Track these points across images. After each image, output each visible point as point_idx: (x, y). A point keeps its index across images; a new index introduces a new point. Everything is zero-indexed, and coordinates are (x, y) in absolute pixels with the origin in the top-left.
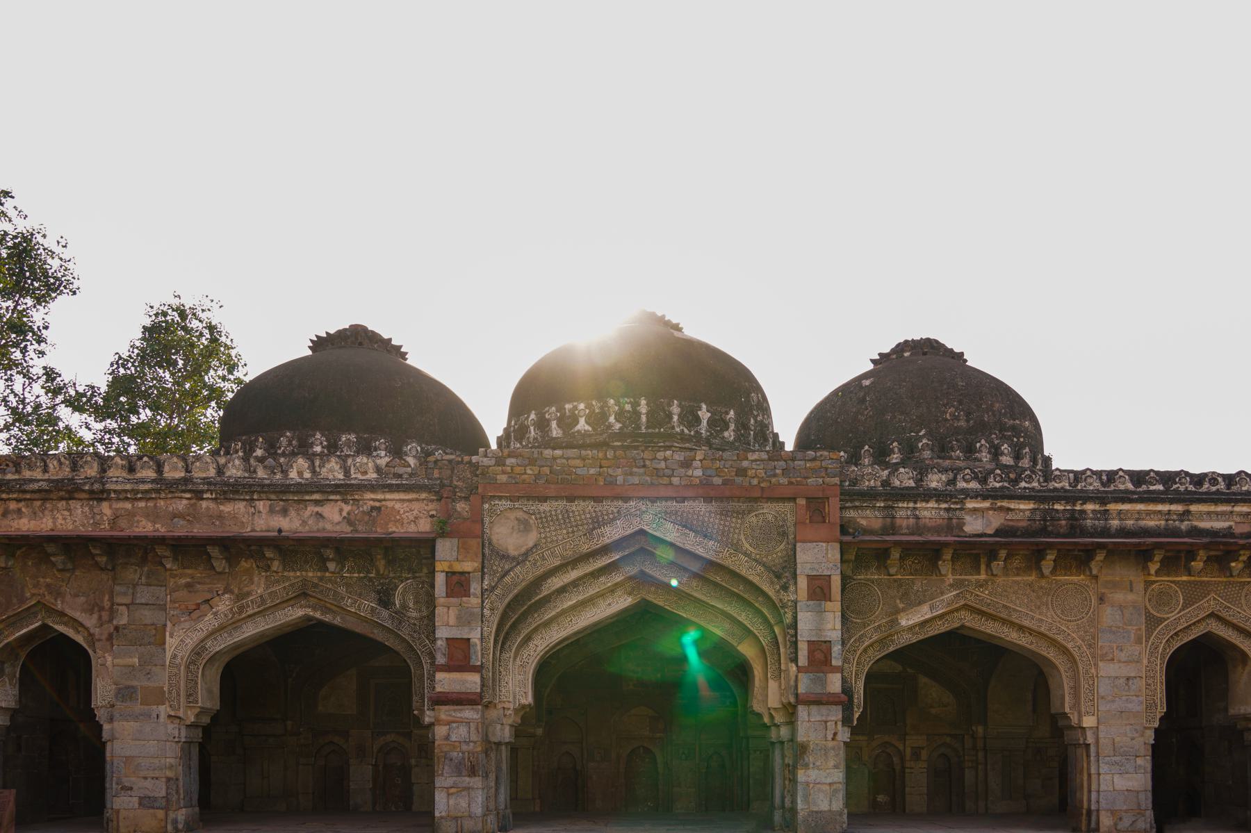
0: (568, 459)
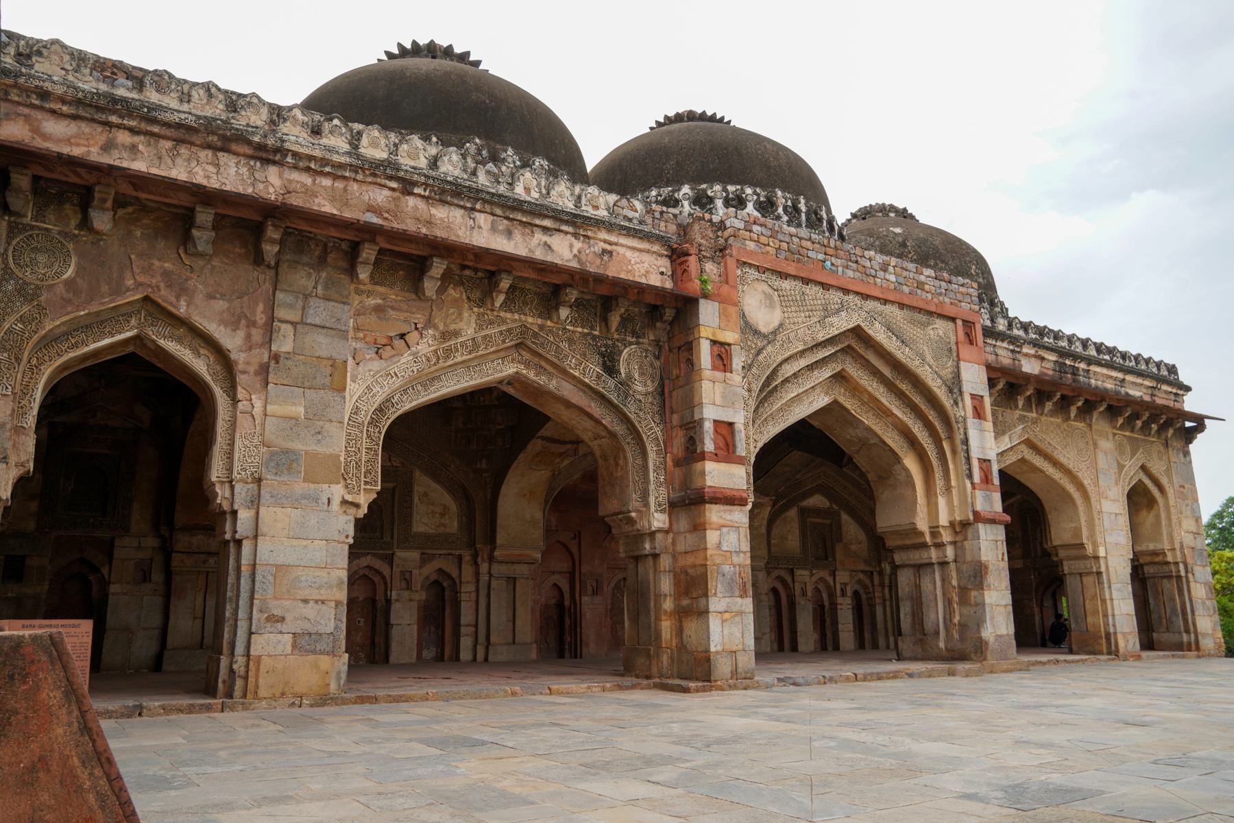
0: (801, 239)
